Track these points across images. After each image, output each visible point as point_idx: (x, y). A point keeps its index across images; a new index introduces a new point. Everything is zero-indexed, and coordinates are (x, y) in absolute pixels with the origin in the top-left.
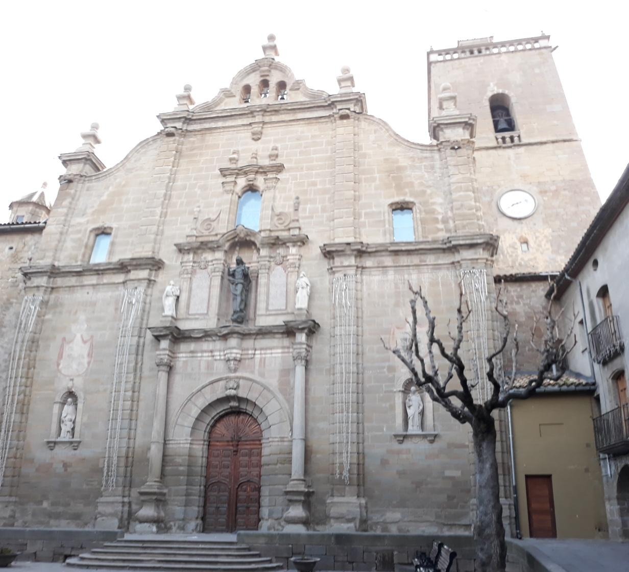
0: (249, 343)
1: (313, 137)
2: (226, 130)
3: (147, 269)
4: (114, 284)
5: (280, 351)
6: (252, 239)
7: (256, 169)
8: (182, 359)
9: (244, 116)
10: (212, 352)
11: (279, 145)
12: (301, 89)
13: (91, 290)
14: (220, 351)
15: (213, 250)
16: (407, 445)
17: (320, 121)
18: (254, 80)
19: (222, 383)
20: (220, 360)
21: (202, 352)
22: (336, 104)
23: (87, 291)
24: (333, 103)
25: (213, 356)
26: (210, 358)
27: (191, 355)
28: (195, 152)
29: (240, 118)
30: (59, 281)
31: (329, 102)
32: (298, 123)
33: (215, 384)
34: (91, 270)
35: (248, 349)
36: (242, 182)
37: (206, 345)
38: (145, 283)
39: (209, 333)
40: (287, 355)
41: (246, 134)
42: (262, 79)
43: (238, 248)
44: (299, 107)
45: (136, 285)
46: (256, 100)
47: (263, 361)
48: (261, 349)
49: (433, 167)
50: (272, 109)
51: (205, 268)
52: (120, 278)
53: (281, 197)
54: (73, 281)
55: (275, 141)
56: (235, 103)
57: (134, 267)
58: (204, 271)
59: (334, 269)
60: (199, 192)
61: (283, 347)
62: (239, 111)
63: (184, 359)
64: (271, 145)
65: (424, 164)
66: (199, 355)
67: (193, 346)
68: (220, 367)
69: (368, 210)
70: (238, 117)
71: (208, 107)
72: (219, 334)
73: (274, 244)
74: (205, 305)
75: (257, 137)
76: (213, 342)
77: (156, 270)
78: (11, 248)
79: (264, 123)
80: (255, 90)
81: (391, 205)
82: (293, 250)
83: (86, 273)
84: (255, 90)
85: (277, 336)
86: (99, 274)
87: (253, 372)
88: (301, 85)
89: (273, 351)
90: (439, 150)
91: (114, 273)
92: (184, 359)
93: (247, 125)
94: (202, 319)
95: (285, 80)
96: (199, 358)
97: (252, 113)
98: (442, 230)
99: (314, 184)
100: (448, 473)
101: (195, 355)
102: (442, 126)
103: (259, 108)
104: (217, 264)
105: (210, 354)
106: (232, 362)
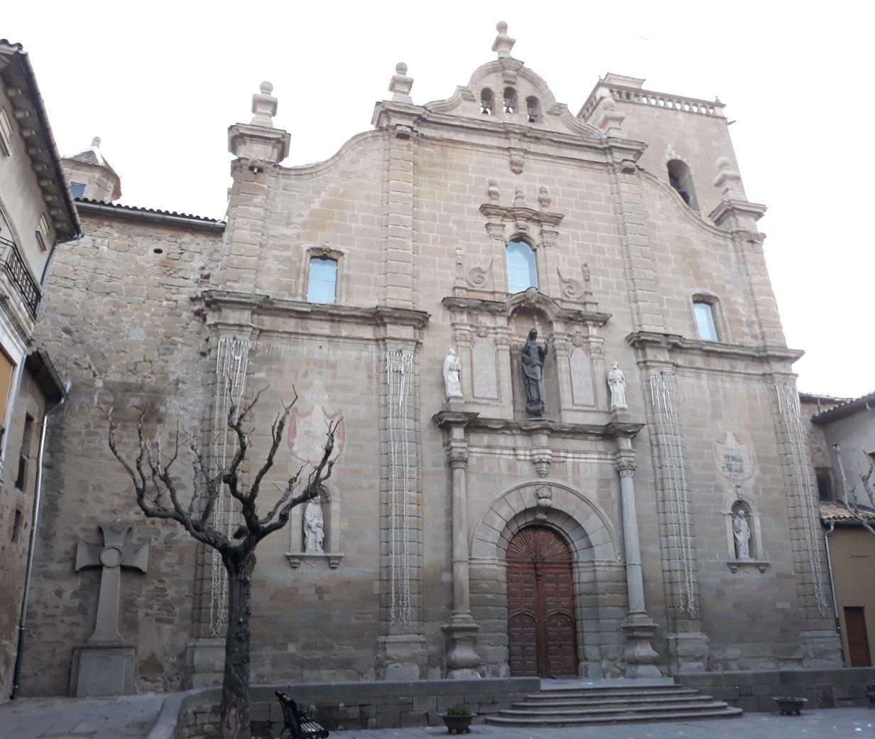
0: (559, 442)
1: (588, 186)
2: (474, 148)
3: (410, 325)
4: (362, 339)
5: (596, 456)
6: (543, 307)
7: (530, 215)
8: (475, 455)
9: (495, 134)
10: (514, 449)
11: (547, 187)
12: (561, 116)
13: (325, 343)
14: (525, 450)
15: (493, 313)
16: (740, 574)
17: (594, 166)
19: (529, 490)
20: (525, 460)
22: (613, 149)
23: (319, 343)
24: (610, 148)
25: (516, 455)
26: (511, 457)
27: (487, 450)
28: (437, 169)
29: (489, 136)
30: (267, 322)
31: (605, 146)
32: (567, 162)
33: (521, 490)
34: (323, 313)
35: (559, 451)
36: (510, 228)
37: (503, 440)
38: (412, 346)
39: (511, 425)
40: (604, 461)
42: (506, 85)
44: (568, 141)
45: (400, 347)
47: (576, 467)
48: (574, 452)
49: (728, 259)
50: (533, 135)
51: (485, 337)
52: (368, 332)
53: (564, 260)
54: (291, 324)
57: (394, 321)
58: (484, 339)
59: (649, 364)
60: (455, 228)
61: (600, 453)
62: (491, 126)
63: (478, 455)
64: (538, 185)
65: (719, 252)
66: (498, 451)
67: (486, 439)
68: (525, 468)
69: (669, 297)
70: (487, 133)
72: (524, 428)
73: (570, 319)
74: (494, 388)
76: (512, 437)
77: (420, 329)
78: (158, 251)
79: (526, 152)
81: (694, 296)
82: (593, 331)
83: (313, 317)
85: (590, 437)
86: (333, 321)
87: (565, 479)
88: (563, 110)
89: (588, 456)
90: (733, 239)
91: (357, 324)
92: (478, 455)
93: (504, 149)
94: (494, 406)
95: (538, 96)
96: (497, 456)
97: (507, 133)
98: (747, 334)
100: (779, 605)
101: (493, 451)
102: (736, 212)
103: (518, 129)
104: (502, 333)
105: (512, 452)
106: (544, 465)
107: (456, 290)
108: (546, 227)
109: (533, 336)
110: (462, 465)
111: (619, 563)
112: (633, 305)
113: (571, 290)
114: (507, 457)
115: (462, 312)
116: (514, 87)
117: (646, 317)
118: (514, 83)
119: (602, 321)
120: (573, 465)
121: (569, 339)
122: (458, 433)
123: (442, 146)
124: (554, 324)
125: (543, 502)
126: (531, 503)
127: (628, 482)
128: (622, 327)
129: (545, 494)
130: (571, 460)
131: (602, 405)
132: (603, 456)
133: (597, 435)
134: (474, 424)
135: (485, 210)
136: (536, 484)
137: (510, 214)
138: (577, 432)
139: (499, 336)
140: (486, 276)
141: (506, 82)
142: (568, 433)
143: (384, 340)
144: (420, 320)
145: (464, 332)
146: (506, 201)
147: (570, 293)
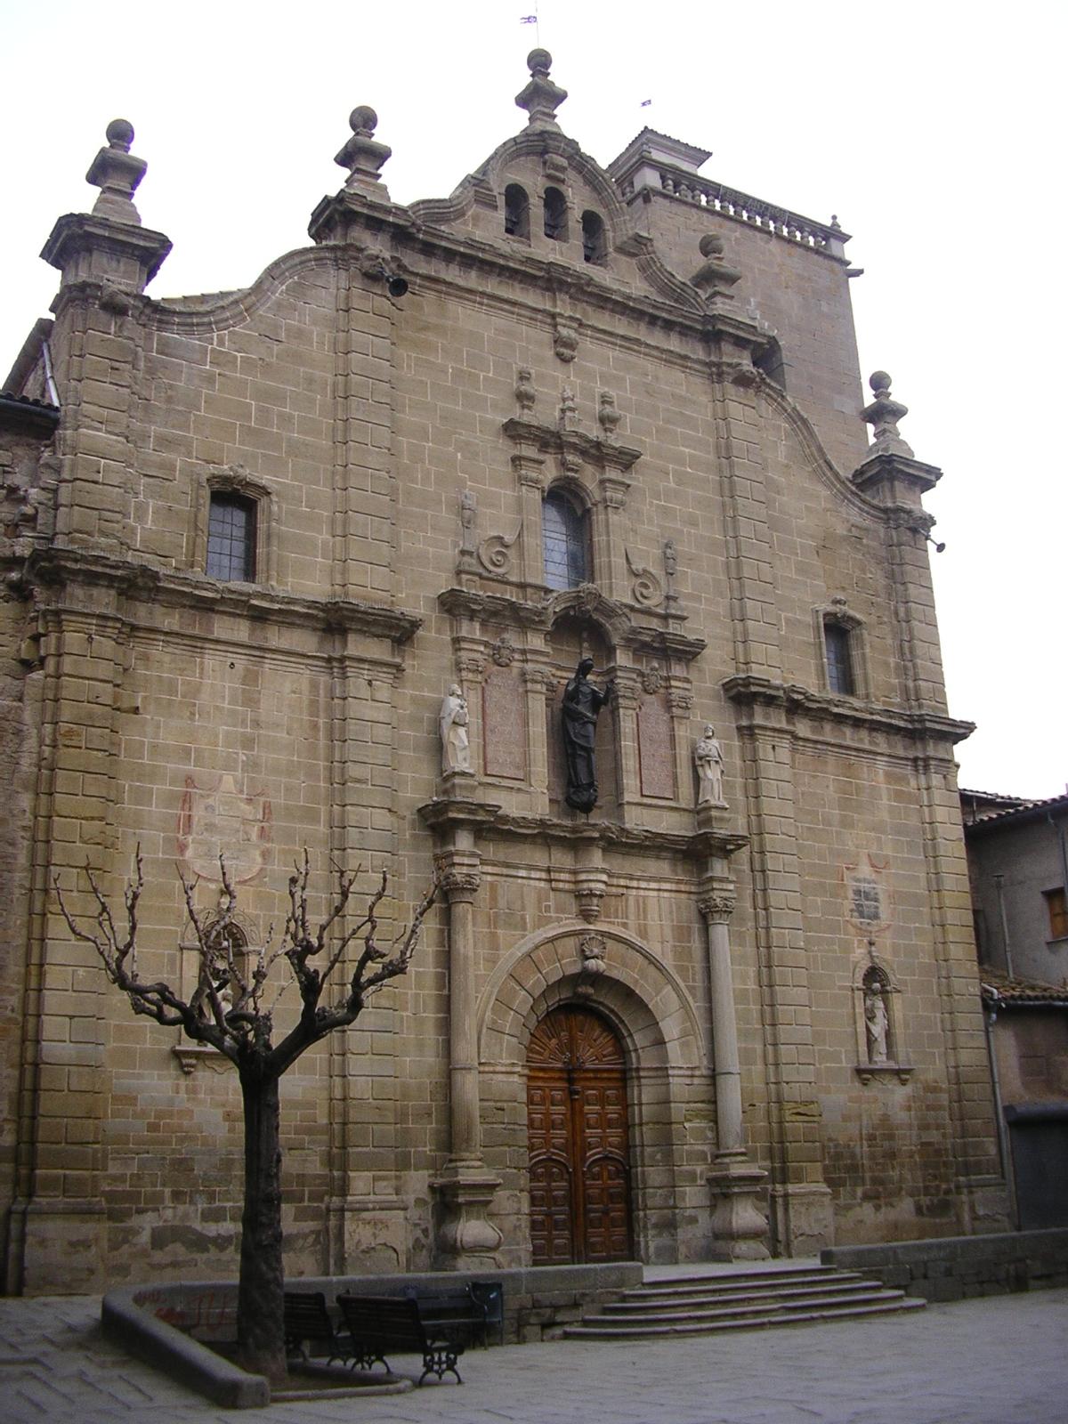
0: (622, 864)
3: (388, 637)
5: (673, 887)
10: (548, 871)
16: (876, 1088)
19: (571, 943)
21: (531, 868)
23: (231, 658)
26: (542, 884)
28: (431, 336)
42: (550, 184)
51: (507, 665)
56: (488, 229)
61: (679, 882)
64: (599, 389)
66: (523, 873)
71: (434, 210)
75: (564, 352)
95: (601, 211)
96: (520, 881)
105: (544, 875)
106: (595, 901)
108: (612, 473)
109: (584, 669)
111: (705, 1072)
112: (739, 625)
113: (645, 592)
114: (537, 883)
115: (471, 619)
116: (562, 188)
117: (757, 651)
118: (563, 181)
121: (639, 679)
122: (464, 841)
123: (440, 292)
124: (618, 651)
125: (592, 964)
127: (720, 933)
128: (716, 665)
129: (596, 951)
131: (686, 800)
132: (683, 887)
133: (677, 851)
134: (493, 828)
135: (513, 430)
137: (550, 441)
138: (652, 845)
139: (529, 666)
140: (512, 553)
141: (549, 177)
143: (342, 660)
144: (401, 632)
146: (544, 416)
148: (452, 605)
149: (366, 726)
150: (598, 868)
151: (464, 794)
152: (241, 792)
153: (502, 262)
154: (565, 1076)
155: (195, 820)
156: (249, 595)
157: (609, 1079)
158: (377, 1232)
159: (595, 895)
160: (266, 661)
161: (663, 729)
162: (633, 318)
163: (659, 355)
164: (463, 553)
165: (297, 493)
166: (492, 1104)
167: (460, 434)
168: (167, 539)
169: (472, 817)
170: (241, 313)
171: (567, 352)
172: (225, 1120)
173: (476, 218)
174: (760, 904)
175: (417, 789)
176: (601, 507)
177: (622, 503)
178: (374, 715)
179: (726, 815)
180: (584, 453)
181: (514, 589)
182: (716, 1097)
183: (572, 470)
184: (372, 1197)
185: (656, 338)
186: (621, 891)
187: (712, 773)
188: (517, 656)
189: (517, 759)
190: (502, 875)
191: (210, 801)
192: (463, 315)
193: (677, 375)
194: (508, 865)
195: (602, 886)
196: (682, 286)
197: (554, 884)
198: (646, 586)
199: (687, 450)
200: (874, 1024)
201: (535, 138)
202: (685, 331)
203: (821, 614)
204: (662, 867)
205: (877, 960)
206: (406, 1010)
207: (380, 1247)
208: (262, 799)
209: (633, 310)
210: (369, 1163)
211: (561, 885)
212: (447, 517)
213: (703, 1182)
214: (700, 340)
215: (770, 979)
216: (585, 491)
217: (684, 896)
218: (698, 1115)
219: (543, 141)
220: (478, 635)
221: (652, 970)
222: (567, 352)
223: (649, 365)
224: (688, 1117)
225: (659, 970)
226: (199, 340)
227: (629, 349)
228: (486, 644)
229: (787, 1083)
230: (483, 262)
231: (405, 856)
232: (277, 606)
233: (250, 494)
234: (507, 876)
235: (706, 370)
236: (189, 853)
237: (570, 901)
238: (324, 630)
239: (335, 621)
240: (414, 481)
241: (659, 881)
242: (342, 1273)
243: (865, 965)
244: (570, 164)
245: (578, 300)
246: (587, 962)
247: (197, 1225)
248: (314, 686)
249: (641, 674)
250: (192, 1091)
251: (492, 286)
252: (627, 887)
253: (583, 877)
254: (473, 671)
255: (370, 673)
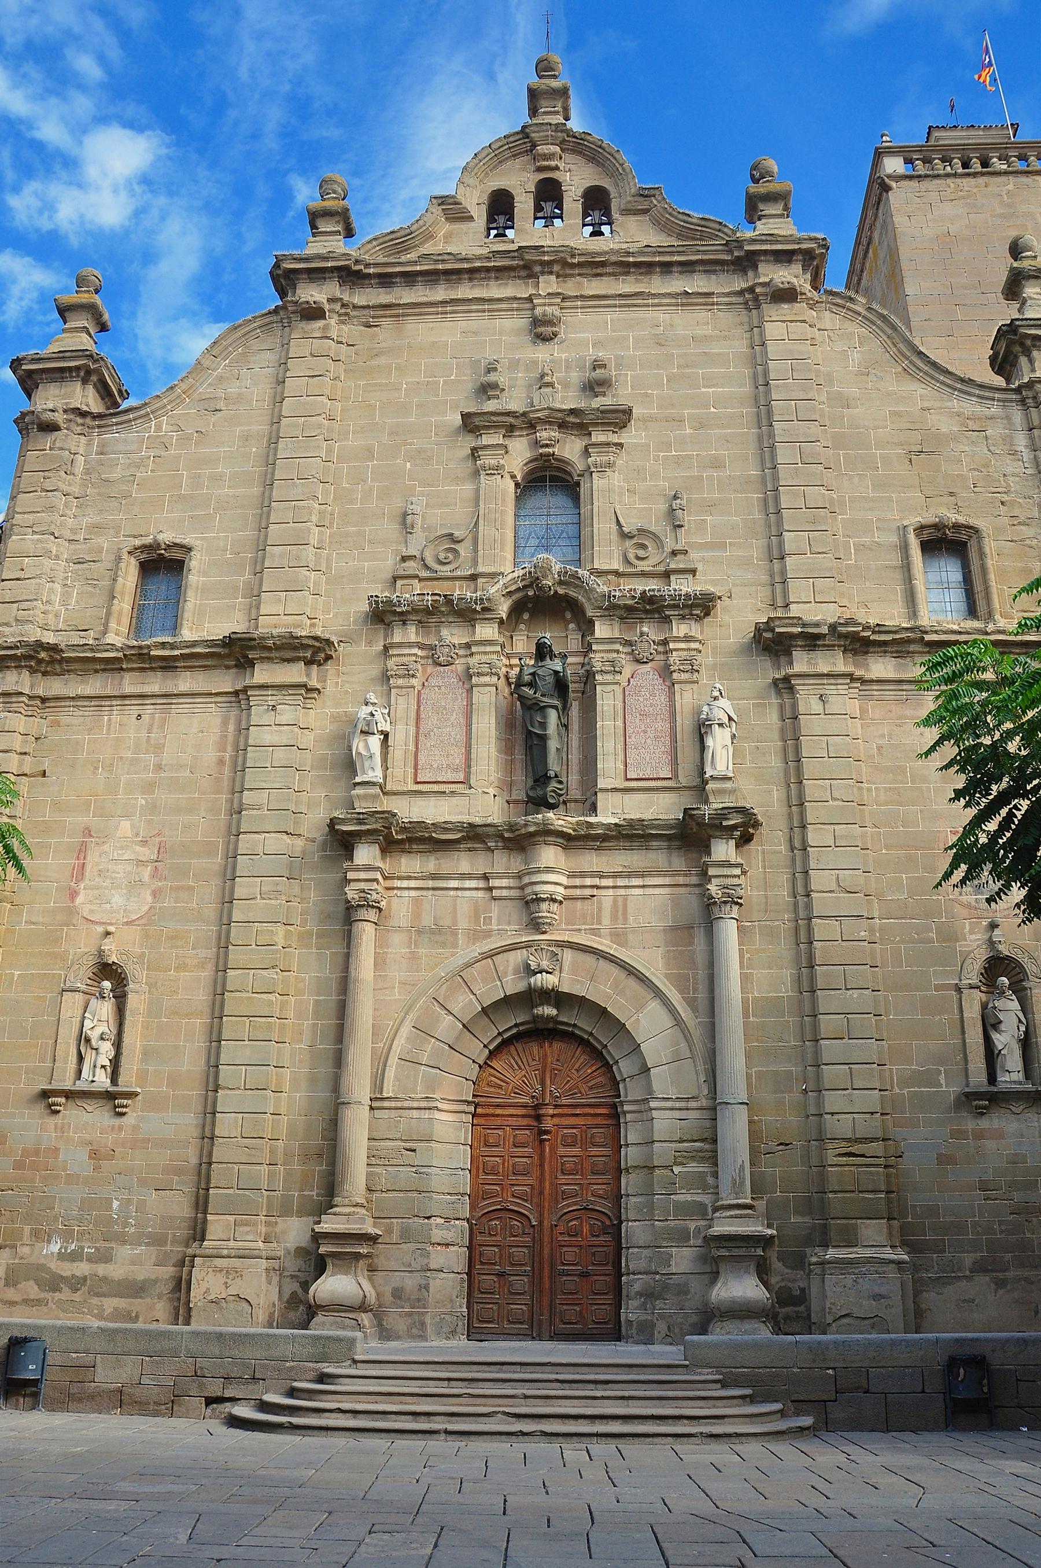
5: (667, 881)
10: (486, 877)
18: (520, 181)
19: (516, 958)
21: (463, 877)
25: (490, 889)
26: (480, 894)
27: (430, 884)
28: (383, 360)
37: (463, 862)
39: (480, 830)
41: (516, 323)
43: (526, 616)
46: (528, 232)
55: (597, 344)
56: (471, 241)
61: (675, 873)
71: (399, 241)
75: (542, 331)
76: (489, 854)
80: (524, 204)
84: (524, 204)
89: (649, 881)
95: (606, 183)
96: (452, 893)
99: (717, 464)
105: (481, 884)
107: (399, 583)
108: (598, 437)
109: (542, 652)
110: (372, 915)
111: (704, 1103)
113: (641, 553)
114: (474, 893)
115: (404, 623)
116: (555, 175)
117: (798, 590)
118: (557, 168)
119: (702, 607)
120: (615, 901)
121: (628, 649)
122: (365, 854)
125: (538, 980)
126: (513, 985)
127: (729, 931)
128: (741, 614)
129: (545, 964)
130: (611, 892)
132: (681, 880)
133: (668, 838)
134: (400, 839)
136: (527, 945)
137: (526, 423)
138: (632, 835)
139: (473, 661)
142: (605, 838)
144: (315, 652)
145: (405, 659)
147: (638, 558)
148: (382, 616)
149: (267, 751)
150: (553, 868)
151: (364, 805)
152: (137, 835)
153: (466, 266)
154: (532, 1113)
155: (88, 867)
156: (148, 647)
157: (585, 1115)
158: (229, 1281)
159: (544, 900)
160: (173, 706)
161: (662, 699)
162: (641, 274)
163: (674, 301)
164: (404, 559)
165: (222, 544)
166: (399, 1143)
167: (412, 444)
168: (88, 614)
169: (364, 828)
170: (179, 396)
171: (547, 330)
172: (90, 1157)
173: (448, 237)
174: (800, 890)
175: (317, 809)
176: (587, 474)
177: (610, 465)
178: (276, 739)
179: (728, 785)
180: (562, 426)
181: (464, 584)
182: (337, 1115)
183: (547, 446)
184: (232, 1244)
185: (658, 284)
186: (588, 892)
187: (719, 741)
188: (461, 652)
189: (458, 761)
190: (428, 889)
191: (105, 847)
192: (421, 330)
193: (702, 315)
194: (434, 877)
195: (561, 890)
196: (703, 223)
197: (495, 893)
198: (643, 547)
199: (711, 390)
200: (999, 1032)
201: (517, 137)
202: (711, 267)
203: (911, 529)
204: (656, 857)
205: (1001, 947)
206: (301, 1042)
207: (232, 1298)
208: (158, 839)
209: (637, 265)
210: (243, 1211)
211: (505, 893)
212: (390, 529)
213: (699, 1242)
214: (734, 272)
215: (812, 984)
216: (569, 464)
217: (682, 890)
218: (693, 1156)
219: (528, 137)
220: (413, 638)
221: (632, 982)
222: (547, 330)
223: (661, 316)
224: (679, 1160)
225: (642, 981)
226: (137, 432)
227: (629, 306)
228: (421, 646)
229: (832, 1114)
230: (447, 272)
231: (308, 879)
232: (177, 652)
233: (177, 555)
234: (434, 889)
235: (740, 300)
236: (79, 900)
237: (514, 910)
238: (236, 666)
239: (238, 652)
240: (351, 502)
241: (643, 876)
242: (187, 1323)
243: (982, 955)
244: (562, 150)
245: (566, 276)
246: (532, 980)
247: (53, 1265)
248: (225, 723)
249: (628, 643)
250: (62, 1129)
251: (465, 291)
252: (598, 887)
253: (526, 880)
254: (404, 676)
255: (274, 698)
